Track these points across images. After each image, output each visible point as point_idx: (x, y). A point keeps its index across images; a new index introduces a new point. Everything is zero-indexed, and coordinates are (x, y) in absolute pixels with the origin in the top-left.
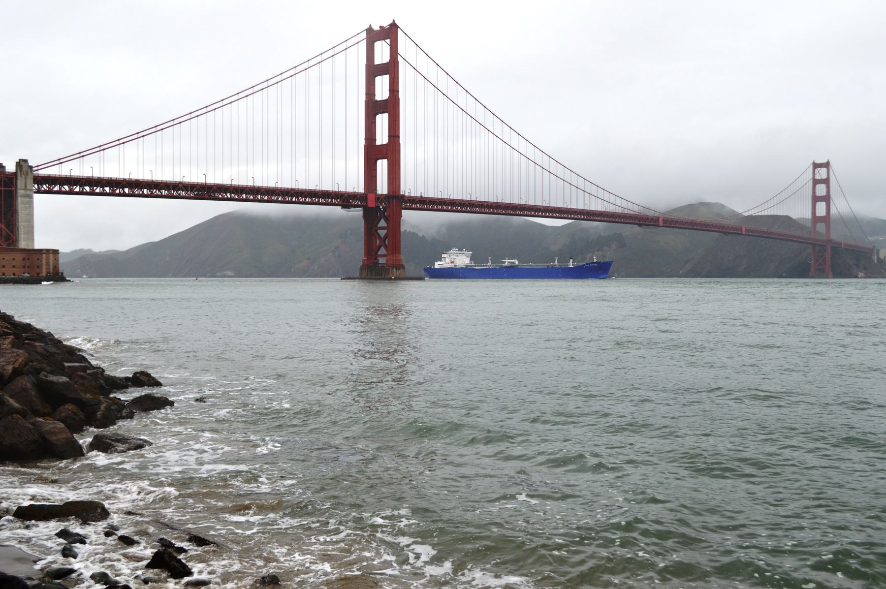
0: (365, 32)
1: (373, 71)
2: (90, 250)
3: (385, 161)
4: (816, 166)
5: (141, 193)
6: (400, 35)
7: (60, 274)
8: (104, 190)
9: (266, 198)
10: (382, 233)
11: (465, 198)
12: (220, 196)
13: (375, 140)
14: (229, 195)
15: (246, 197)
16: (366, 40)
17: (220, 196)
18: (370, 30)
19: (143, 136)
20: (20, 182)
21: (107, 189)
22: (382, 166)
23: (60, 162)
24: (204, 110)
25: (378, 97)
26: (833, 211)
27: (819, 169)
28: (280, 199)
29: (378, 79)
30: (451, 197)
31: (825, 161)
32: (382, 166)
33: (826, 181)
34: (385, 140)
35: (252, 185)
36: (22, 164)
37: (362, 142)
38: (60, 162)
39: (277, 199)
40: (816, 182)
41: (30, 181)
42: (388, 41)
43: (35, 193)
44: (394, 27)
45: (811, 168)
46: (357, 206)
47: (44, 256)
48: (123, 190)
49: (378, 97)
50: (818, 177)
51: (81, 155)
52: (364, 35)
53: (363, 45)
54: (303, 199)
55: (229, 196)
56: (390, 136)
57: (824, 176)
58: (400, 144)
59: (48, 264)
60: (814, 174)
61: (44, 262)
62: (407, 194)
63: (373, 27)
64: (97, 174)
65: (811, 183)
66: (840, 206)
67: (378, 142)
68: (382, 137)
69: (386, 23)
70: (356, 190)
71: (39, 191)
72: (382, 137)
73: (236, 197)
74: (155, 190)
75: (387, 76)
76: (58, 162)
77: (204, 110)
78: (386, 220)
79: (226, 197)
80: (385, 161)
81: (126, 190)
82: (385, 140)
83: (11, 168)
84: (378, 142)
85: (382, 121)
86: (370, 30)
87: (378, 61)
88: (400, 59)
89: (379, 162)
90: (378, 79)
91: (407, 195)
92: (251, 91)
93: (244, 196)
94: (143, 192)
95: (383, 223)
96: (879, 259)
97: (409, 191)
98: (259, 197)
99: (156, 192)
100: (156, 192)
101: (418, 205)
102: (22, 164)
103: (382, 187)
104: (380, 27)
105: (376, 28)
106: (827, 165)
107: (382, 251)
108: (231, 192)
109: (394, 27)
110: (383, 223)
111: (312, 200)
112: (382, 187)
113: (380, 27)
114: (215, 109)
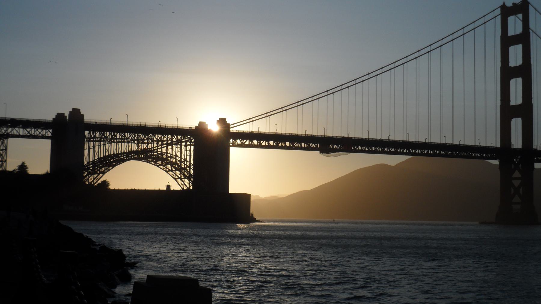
0: (500, 8)
3: (519, 120)
5: (299, 146)
6: (531, 9)
7: (251, 216)
8: (269, 143)
10: (516, 183)
13: (509, 101)
16: (500, 16)
17: (367, 149)
19: (318, 98)
21: (272, 143)
22: (517, 124)
23: (251, 120)
24: (367, 77)
25: (512, 64)
28: (405, 151)
29: (512, 49)
32: (517, 124)
34: (520, 101)
37: (499, 103)
38: (251, 120)
42: (520, 16)
43: (231, 146)
49: (512, 64)
51: (268, 115)
52: (498, 11)
53: (499, 19)
54: (426, 151)
56: (524, 97)
67: (513, 103)
68: (516, 98)
70: (493, 145)
71: (234, 146)
72: (516, 98)
74: (311, 144)
77: (367, 77)
80: (519, 120)
81: (288, 144)
82: (520, 101)
84: (513, 103)
87: (511, 33)
88: (530, 31)
89: (514, 121)
90: (512, 49)
92: (405, 60)
93: (373, 148)
94: (301, 145)
95: (517, 174)
98: (386, 149)
99: (312, 145)
100: (312, 145)
103: (517, 142)
104: (513, 4)
105: (509, 4)
107: (517, 199)
110: (517, 174)
111: (434, 152)
112: (517, 142)
113: (513, 4)
114: (377, 75)
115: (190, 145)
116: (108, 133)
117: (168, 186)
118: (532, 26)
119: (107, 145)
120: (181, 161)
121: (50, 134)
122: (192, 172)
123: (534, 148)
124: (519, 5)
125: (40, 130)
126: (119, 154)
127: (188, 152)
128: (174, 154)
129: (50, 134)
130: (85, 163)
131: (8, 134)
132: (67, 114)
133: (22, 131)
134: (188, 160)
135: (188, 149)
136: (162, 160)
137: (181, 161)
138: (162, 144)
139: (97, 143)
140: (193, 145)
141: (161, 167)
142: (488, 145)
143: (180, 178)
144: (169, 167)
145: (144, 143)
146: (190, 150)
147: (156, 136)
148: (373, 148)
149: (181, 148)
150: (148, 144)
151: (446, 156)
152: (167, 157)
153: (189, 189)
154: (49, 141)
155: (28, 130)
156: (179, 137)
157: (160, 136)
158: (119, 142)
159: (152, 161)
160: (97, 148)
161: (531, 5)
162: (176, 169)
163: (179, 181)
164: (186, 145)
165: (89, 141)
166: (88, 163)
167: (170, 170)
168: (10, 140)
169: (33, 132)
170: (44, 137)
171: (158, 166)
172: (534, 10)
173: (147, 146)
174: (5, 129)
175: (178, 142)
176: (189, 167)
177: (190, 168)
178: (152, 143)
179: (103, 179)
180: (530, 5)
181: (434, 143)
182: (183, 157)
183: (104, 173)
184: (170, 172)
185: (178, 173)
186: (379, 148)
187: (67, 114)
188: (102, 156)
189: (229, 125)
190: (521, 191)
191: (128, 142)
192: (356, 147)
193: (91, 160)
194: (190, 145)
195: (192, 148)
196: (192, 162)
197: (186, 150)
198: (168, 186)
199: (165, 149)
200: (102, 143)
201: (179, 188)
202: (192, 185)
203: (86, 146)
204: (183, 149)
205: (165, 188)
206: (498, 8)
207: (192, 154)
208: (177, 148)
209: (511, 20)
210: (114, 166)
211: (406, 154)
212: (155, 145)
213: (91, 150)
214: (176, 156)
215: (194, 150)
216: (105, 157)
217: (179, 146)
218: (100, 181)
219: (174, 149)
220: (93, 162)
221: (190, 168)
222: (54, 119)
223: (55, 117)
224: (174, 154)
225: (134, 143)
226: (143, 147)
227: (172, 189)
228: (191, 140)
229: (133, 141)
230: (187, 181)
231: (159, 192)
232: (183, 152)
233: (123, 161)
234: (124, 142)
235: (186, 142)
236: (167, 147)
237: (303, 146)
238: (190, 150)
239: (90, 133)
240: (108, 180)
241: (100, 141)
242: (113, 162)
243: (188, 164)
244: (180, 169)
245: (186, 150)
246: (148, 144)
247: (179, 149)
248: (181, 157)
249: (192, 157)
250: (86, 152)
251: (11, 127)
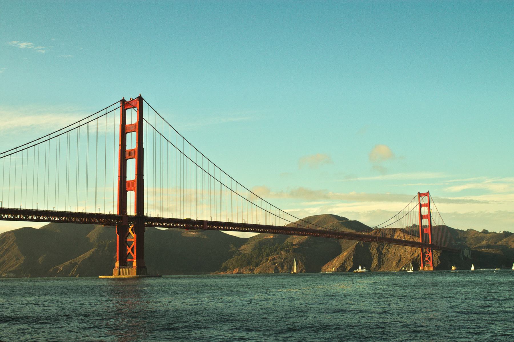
1: (124, 130)
4: (420, 195)
6: (145, 104)
12: (12, 217)
14: (18, 217)
15: (32, 218)
17: (12, 217)
18: (123, 101)
22: (131, 197)
25: (128, 148)
26: (433, 225)
27: (423, 197)
31: (427, 192)
32: (131, 197)
33: (428, 205)
39: (55, 219)
40: (421, 206)
42: (136, 109)
44: (141, 99)
45: (417, 197)
50: (422, 203)
52: (119, 104)
53: (119, 112)
55: (18, 217)
57: (426, 202)
58: (144, 180)
60: (420, 201)
63: (125, 99)
66: (437, 222)
68: (131, 175)
69: (135, 96)
72: (131, 175)
73: (24, 218)
75: (136, 132)
79: (16, 218)
84: (128, 179)
85: (131, 164)
86: (123, 101)
87: (128, 122)
88: (144, 121)
91: (148, 216)
92: (37, 142)
96: (464, 256)
97: (150, 213)
103: (131, 211)
104: (130, 99)
105: (127, 99)
106: (428, 194)
109: (141, 99)
112: (131, 211)
118: (145, 116)
123: (144, 215)
124: (135, 100)
148: (30, 217)
151: (70, 222)
161: (144, 100)
172: (148, 105)
180: (144, 100)
181: (41, 210)
186: (23, 217)
192: (3, 215)
206: (119, 102)
209: (128, 112)
211: (46, 221)
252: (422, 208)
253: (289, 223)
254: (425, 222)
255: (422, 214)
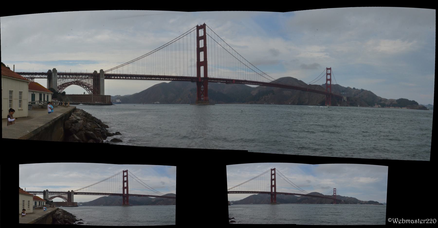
2: (120, 96)
9: (168, 79)
10: (202, 89)
11: (227, 78)
20: (101, 76)
26: (332, 83)
28: (172, 79)
30: (223, 78)
35: (164, 75)
36: (102, 71)
41: (104, 75)
46: (195, 81)
47: (107, 97)
48: (128, 77)
50: (328, 73)
57: (330, 73)
59: (108, 100)
61: (107, 99)
62: (209, 77)
64: (121, 73)
65: (326, 75)
70: (194, 76)
76: (111, 70)
78: (203, 86)
83: (98, 72)
93: (162, 79)
95: (202, 87)
98: (166, 79)
101: (213, 81)
102: (102, 71)
108: (158, 78)
110: (202, 87)
115: (91, 79)
116: (65, 76)
117: (84, 93)
119: (65, 80)
120: (88, 85)
121: (47, 77)
122: (92, 88)
125: (44, 76)
126: (68, 82)
127: (91, 81)
128: (86, 82)
129: (47, 77)
130: (58, 86)
131: (34, 77)
132: (52, 70)
133: (38, 76)
134: (91, 84)
135: (91, 80)
136: (82, 84)
137: (88, 85)
138: (82, 79)
139: (61, 79)
140: (93, 79)
141: (82, 86)
142: (193, 76)
143: (88, 90)
144: (85, 86)
145: (76, 79)
146: (91, 81)
147: (80, 76)
148: (162, 79)
149: (88, 80)
150: (78, 79)
152: (84, 83)
153: (91, 94)
154: (47, 79)
155: (40, 76)
156: (88, 76)
157: (81, 76)
158: (68, 79)
159: (79, 85)
160: (61, 81)
162: (87, 87)
163: (88, 91)
164: (90, 79)
165: (59, 78)
166: (59, 86)
167: (85, 88)
168: (35, 79)
169: (41, 76)
170: (45, 78)
171: (81, 86)
173: (77, 80)
174: (33, 76)
175: (87, 78)
176: (91, 86)
177: (91, 87)
178: (79, 78)
179: (63, 91)
182: (89, 83)
183: (64, 89)
184: (85, 88)
185: (87, 88)
187: (52, 70)
188: (63, 83)
189: (104, 72)
190: (204, 93)
191: (71, 79)
193: (60, 85)
194: (91, 79)
195: (92, 80)
196: (92, 85)
197: (90, 81)
198: (84, 93)
199: (83, 80)
200: (63, 79)
201: (89, 94)
202: (92, 92)
203: (58, 80)
204: (89, 80)
205: (83, 94)
207: (92, 82)
208: (87, 80)
210: (67, 87)
212: (80, 79)
213: (60, 82)
214: (87, 83)
215: (93, 81)
216: (63, 84)
217: (87, 79)
218: (62, 92)
219: (86, 80)
220: (60, 86)
221: (91, 87)
222: (48, 72)
223: (48, 71)
224: (86, 82)
225: (73, 79)
226: (76, 80)
227: (86, 94)
228: (92, 78)
229: (73, 78)
230: (90, 91)
231: (81, 95)
232: (89, 81)
233: (70, 85)
234: (70, 79)
235: (90, 78)
236: (84, 80)
237: (134, 78)
238: (91, 81)
239: (59, 76)
240: (65, 91)
241: (62, 78)
242: (67, 85)
243: (91, 85)
244: (88, 87)
245: (90, 81)
246: (78, 79)
247: (87, 80)
248: (88, 83)
249: (92, 83)
250: (58, 82)
251: (35, 75)
252: (328, 75)
253: (271, 81)
254: (329, 82)
255: (328, 78)
